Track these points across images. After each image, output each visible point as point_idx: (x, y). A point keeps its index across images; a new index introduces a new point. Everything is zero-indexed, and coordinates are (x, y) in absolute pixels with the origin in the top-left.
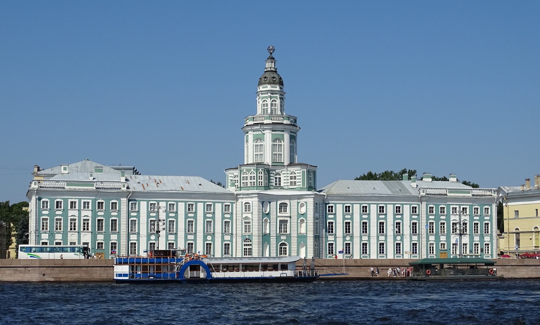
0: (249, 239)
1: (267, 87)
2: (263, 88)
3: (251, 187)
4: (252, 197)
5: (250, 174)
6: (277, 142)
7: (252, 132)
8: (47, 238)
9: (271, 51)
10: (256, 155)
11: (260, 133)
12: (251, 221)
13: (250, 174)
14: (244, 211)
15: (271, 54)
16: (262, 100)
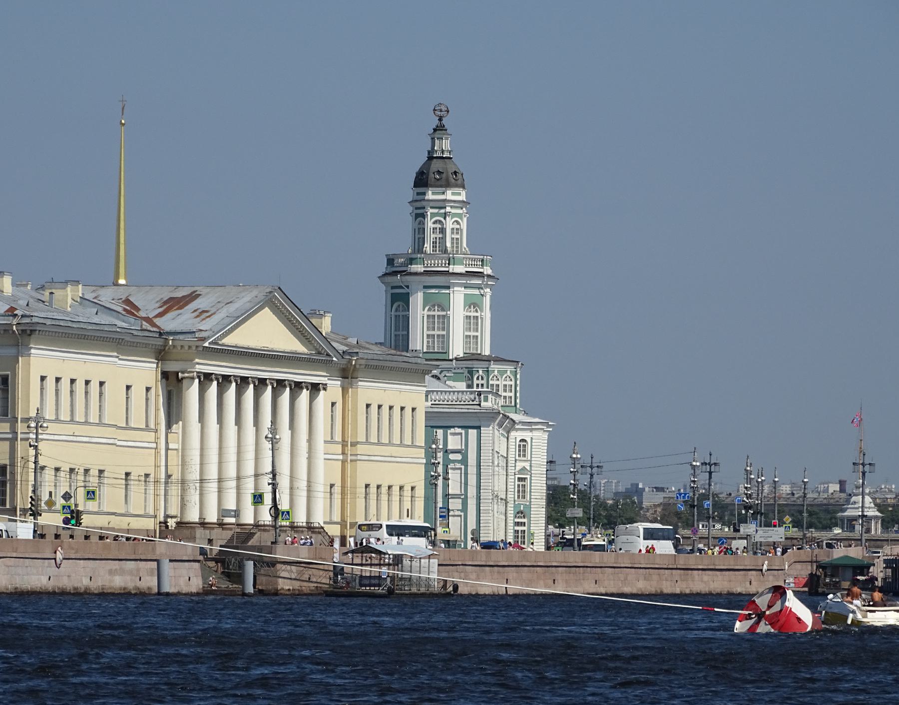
0: (522, 513)
1: (459, 194)
2: (453, 194)
3: (508, 406)
4: (531, 430)
5: (504, 380)
6: (434, 310)
7: (463, 288)
8: (461, 508)
9: (441, 113)
10: (428, 336)
11: (476, 292)
12: (528, 477)
13: (504, 380)
14: (517, 458)
15: (440, 119)
16: (451, 219)
